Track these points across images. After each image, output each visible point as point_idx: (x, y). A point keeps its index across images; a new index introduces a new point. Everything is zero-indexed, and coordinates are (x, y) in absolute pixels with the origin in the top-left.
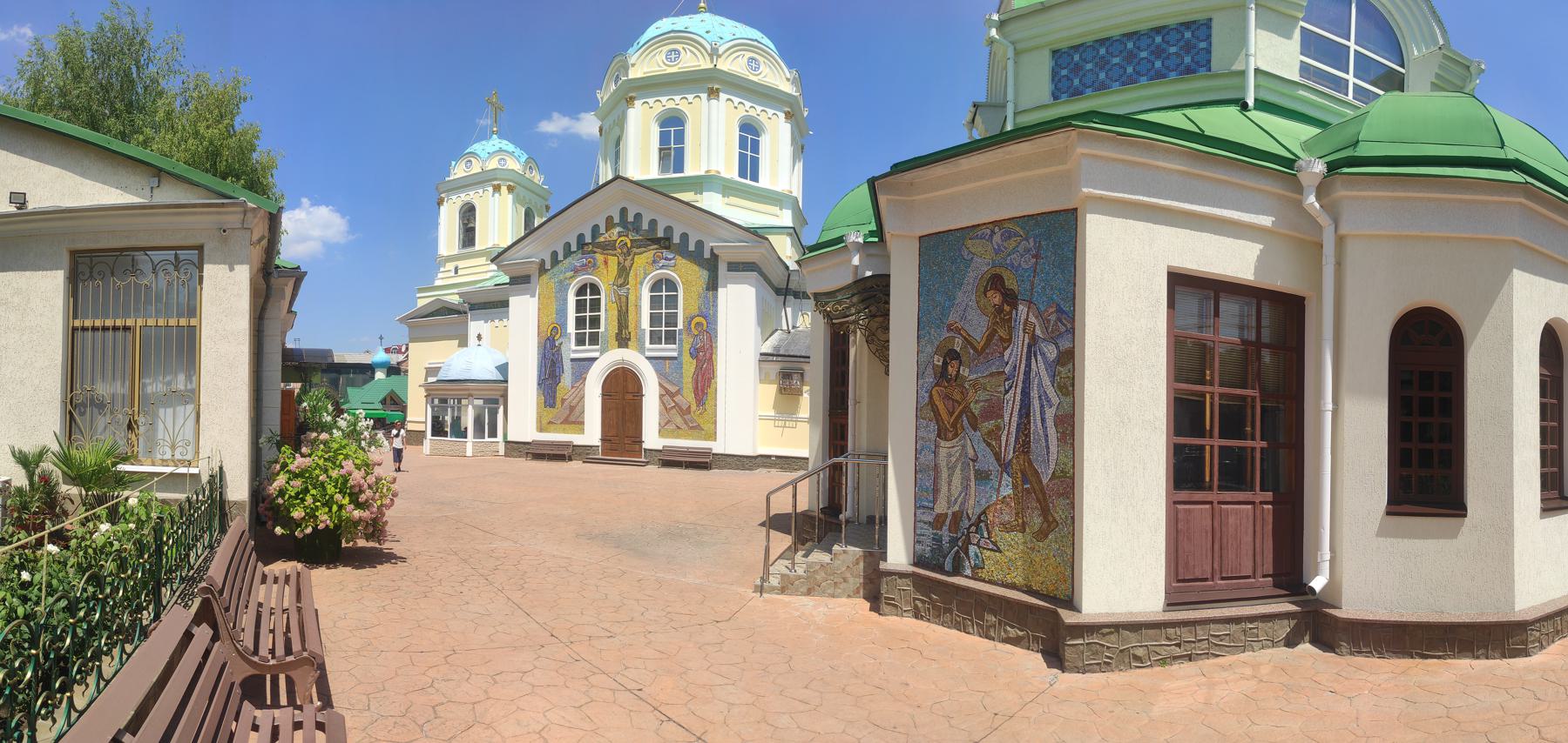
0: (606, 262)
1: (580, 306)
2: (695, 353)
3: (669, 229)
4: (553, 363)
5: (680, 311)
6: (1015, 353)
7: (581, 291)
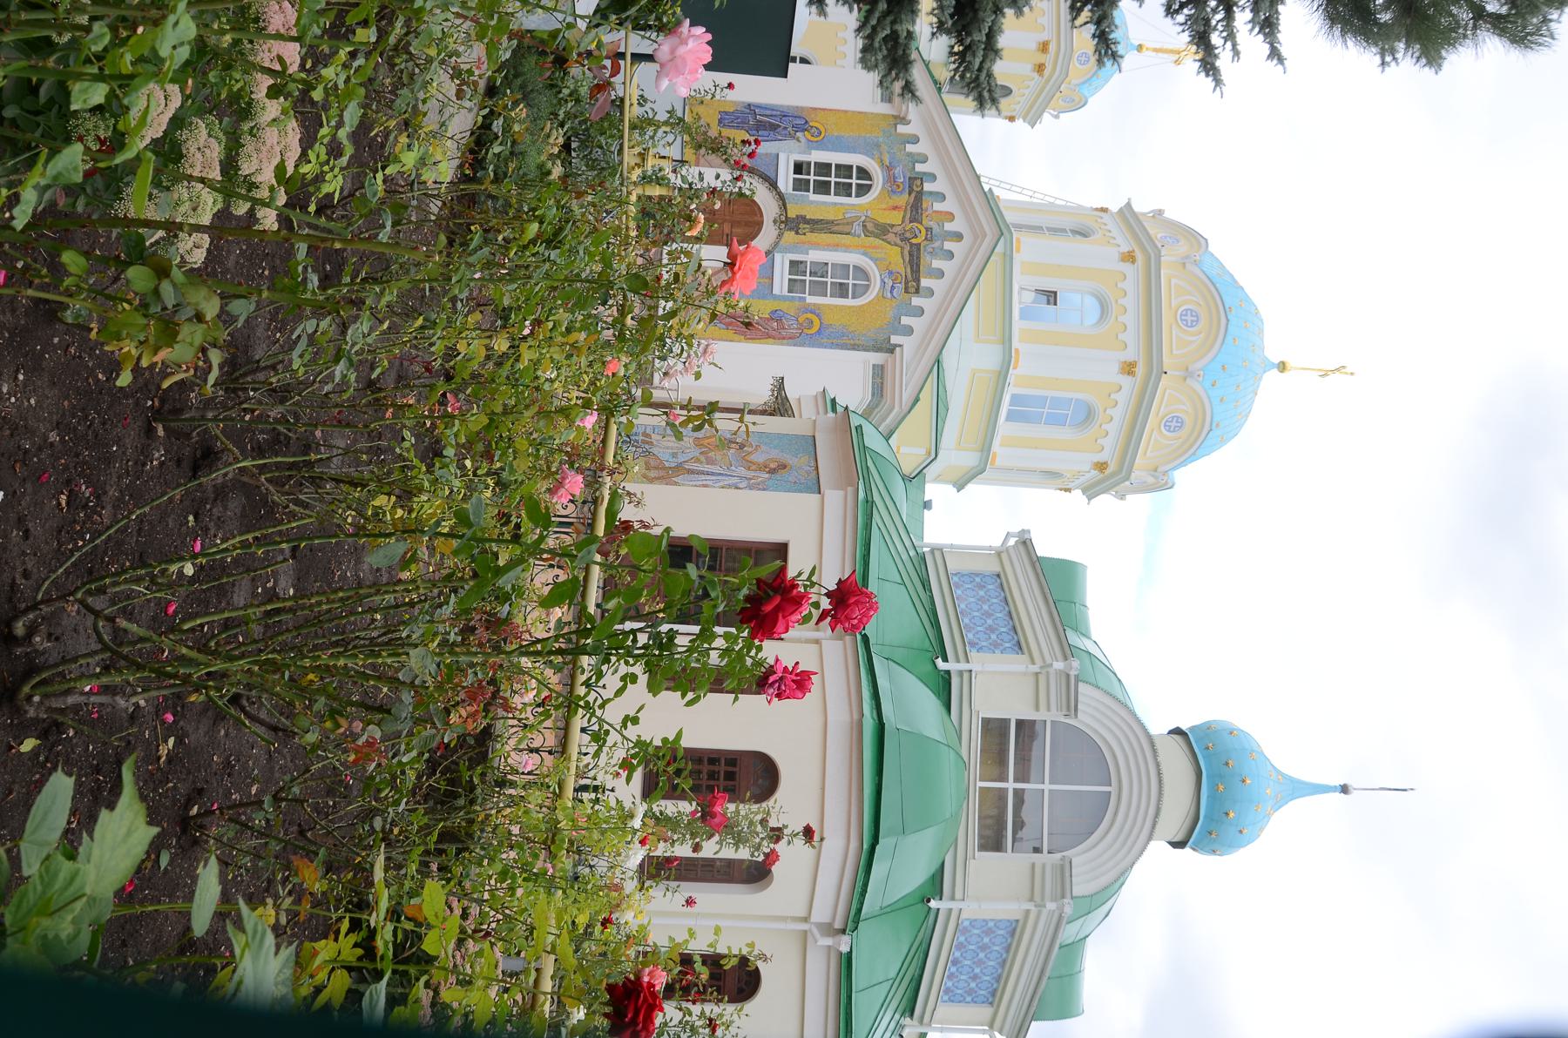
0: (895, 208)
1: (844, 170)
2: (776, 317)
5: (828, 300)
6: (742, 471)
7: (863, 173)
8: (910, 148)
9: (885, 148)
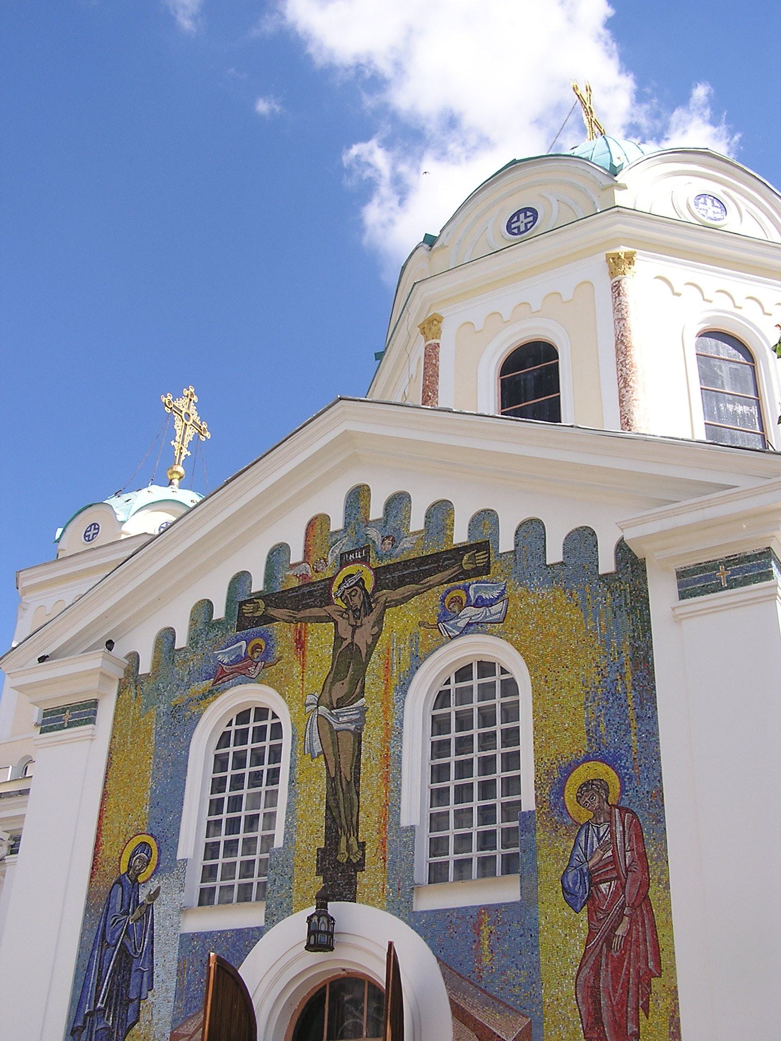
0: (300, 644)
2: (581, 890)
3: (486, 519)
4: (125, 960)
8: (181, 642)
9: (179, 697)
